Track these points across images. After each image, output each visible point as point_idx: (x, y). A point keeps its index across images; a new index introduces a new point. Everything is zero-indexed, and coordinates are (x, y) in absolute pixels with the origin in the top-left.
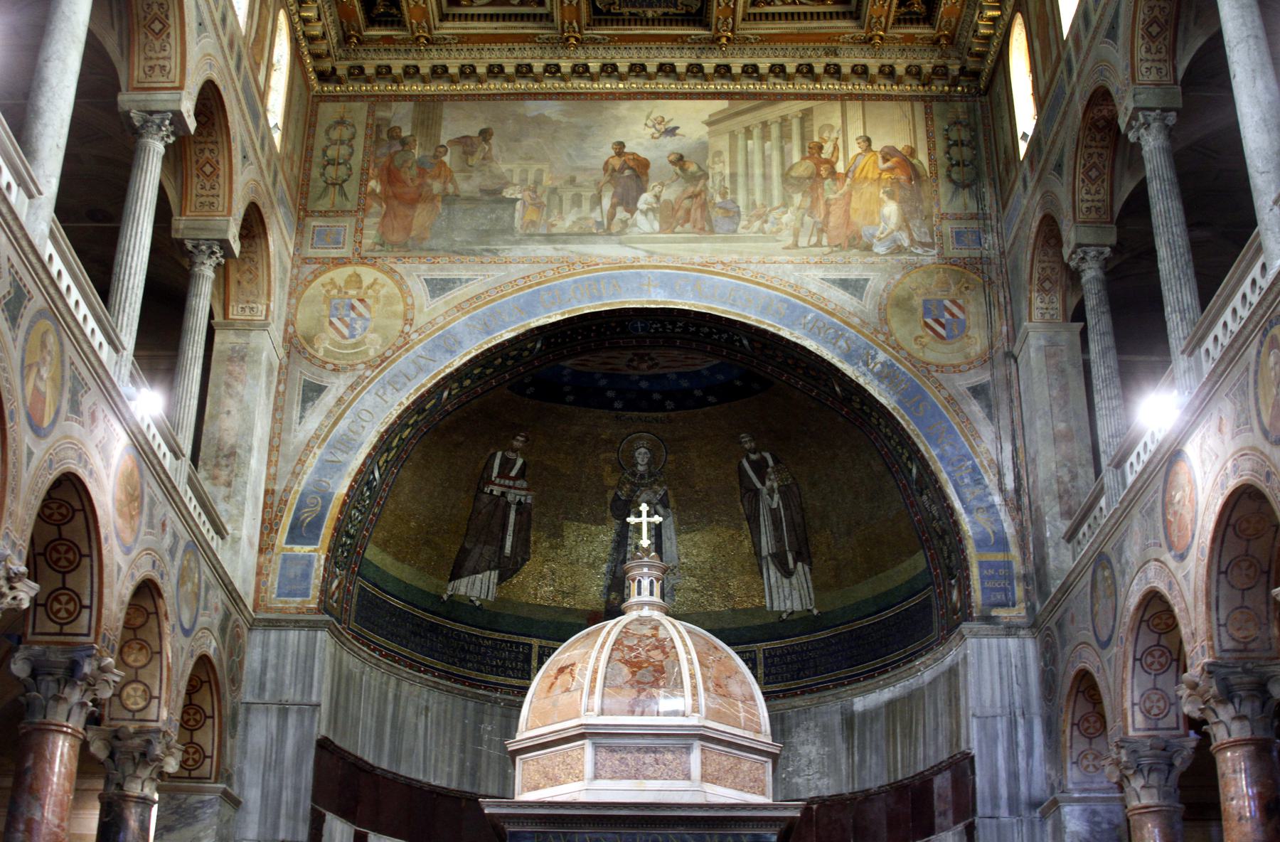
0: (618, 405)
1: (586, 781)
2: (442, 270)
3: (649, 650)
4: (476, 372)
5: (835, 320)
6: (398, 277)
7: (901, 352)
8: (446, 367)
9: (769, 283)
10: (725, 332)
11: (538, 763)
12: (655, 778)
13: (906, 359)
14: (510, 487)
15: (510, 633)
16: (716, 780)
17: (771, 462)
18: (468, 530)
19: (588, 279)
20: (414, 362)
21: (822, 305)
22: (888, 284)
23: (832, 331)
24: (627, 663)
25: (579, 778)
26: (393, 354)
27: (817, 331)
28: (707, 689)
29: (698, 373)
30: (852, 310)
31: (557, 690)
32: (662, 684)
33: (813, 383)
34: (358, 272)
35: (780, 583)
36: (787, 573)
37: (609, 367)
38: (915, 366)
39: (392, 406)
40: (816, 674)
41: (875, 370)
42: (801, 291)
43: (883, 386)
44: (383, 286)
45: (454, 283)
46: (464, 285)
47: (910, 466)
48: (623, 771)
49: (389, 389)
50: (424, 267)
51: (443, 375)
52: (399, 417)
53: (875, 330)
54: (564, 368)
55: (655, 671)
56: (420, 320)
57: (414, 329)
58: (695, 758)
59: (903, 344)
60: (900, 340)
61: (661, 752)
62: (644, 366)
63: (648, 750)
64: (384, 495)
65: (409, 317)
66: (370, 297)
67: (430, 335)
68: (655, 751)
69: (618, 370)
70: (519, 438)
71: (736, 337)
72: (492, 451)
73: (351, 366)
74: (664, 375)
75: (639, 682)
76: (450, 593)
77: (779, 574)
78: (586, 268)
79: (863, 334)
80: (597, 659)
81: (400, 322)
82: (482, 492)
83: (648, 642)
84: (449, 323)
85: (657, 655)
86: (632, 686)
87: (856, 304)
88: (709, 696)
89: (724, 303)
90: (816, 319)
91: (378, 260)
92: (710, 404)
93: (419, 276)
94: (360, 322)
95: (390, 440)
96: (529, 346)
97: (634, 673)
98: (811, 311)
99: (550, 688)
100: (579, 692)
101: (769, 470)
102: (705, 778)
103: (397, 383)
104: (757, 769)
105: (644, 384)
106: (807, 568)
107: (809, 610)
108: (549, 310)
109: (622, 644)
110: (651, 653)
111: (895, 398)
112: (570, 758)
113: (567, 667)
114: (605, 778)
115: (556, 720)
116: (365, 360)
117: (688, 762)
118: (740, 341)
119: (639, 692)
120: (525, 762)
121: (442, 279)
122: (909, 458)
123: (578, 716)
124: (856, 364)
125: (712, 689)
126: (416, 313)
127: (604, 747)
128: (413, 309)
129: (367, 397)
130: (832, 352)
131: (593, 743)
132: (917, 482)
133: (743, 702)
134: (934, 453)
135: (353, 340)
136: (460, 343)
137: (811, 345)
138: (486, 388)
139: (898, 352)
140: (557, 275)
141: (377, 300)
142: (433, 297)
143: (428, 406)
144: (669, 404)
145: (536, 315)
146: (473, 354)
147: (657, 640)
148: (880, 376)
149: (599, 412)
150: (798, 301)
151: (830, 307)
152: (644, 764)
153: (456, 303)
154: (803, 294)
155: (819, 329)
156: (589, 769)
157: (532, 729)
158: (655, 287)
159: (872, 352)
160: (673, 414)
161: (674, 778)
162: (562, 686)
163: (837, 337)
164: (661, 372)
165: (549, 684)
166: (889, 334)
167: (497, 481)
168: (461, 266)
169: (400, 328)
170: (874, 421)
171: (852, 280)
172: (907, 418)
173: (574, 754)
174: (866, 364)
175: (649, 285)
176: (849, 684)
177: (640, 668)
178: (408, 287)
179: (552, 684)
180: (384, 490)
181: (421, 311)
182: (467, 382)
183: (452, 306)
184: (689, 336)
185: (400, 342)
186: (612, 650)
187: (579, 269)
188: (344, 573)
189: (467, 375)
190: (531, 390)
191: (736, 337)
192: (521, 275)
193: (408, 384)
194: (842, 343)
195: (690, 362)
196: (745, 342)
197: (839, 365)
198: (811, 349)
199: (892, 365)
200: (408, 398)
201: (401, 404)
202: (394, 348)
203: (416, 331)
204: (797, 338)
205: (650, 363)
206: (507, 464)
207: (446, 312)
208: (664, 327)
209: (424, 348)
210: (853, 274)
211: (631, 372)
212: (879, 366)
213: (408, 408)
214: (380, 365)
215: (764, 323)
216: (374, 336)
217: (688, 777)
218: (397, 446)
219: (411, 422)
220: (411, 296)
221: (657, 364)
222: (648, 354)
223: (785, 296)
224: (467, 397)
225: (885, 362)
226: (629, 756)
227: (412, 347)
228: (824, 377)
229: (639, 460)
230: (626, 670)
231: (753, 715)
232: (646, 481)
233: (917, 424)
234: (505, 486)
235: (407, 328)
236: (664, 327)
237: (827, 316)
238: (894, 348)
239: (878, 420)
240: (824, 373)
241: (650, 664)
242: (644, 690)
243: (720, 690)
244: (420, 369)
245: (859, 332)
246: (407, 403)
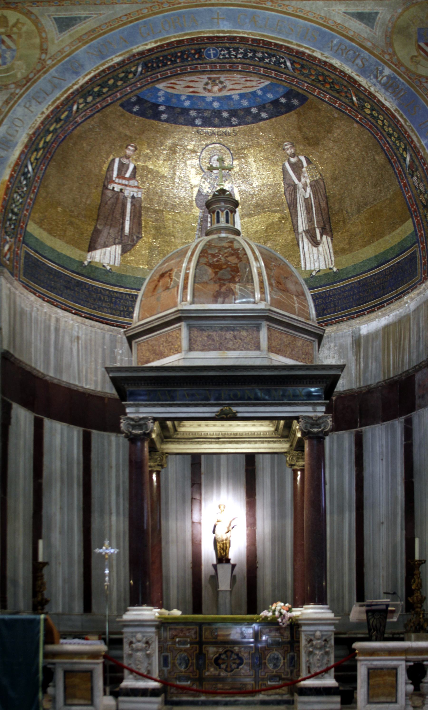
0: (198, 122)
1: (183, 353)
2: (66, 11)
3: (227, 257)
4: (96, 89)
5: (354, 44)
6: (33, 17)
7: (401, 68)
8: (74, 84)
9: (305, 16)
10: (274, 56)
11: (148, 344)
12: (234, 350)
13: (404, 73)
15: (132, 289)
16: (278, 352)
18: (98, 215)
19: (173, 15)
20: (49, 81)
21: (345, 33)
22: (393, 16)
23: (351, 52)
24: (210, 265)
25: (178, 351)
26: (35, 76)
27: (340, 52)
28: (270, 285)
29: (254, 94)
30: (366, 36)
31: (160, 290)
32: (237, 280)
33: (337, 95)
34: (5, 15)
37: (191, 90)
38: (411, 79)
39: (36, 115)
40: (335, 312)
41: (382, 81)
42: (330, 22)
43: (388, 94)
44: (24, 24)
45: (76, 20)
46: (83, 22)
47: (405, 156)
48: (210, 344)
49: (34, 102)
50: (52, 9)
51: (71, 91)
52: (42, 123)
53: (383, 51)
54: (159, 90)
55: (232, 271)
56: (53, 49)
57: (48, 56)
58: (264, 334)
59: (403, 61)
60: (401, 58)
61: (238, 330)
63: (228, 329)
64: (37, 185)
65: (45, 47)
66: (14, 33)
67: (60, 61)
68: (234, 329)
69: (197, 92)
71: (282, 60)
72: (111, 157)
73: (5, 86)
74: (229, 98)
75: (220, 279)
78: (172, 7)
79: (375, 55)
80: (188, 268)
81: (38, 51)
83: (226, 251)
84: (73, 51)
85: (233, 260)
86: (215, 282)
87: (369, 31)
88: (272, 289)
89: (273, 31)
90: (340, 43)
91: (19, 4)
92: (264, 119)
93: (49, 16)
94: (9, 53)
95: (37, 141)
96: (133, 70)
97: (216, 273)
98: (337, 37)
99: (155, 289)
100: (176, 289)
102: (270, 349)
103: (39, 97)
104: (307, 346)
105: (216, 105)
108: (145, 39)
109: (206, 252)
110: (229, 259)
111: (396, 102)
112: (171, 338)
113: (166, 272)
114: (197, 350)
115: (160, 310)
116: (15, 81)
117: (258, 338)
118: (285, 63)
119: (221, 286)
120: (138, 344)
121: (66, 18)
122: (405, 150)
123: (176, 306)
124: (369, 77)
125: (274, 285)
126: (49, 44)
127: (196, 327)
128: (47, 41)
129: (18, 108)
130: (352, 68)
131: (188, 325)
132: (410, 167)
133: (297, 296)
134: (423, 143)
135: (5, 67)
136: (82, 66)
137: (336, 62)
138: (104, 104)
139: (399, 68)
140: (151, 12)
141: (20, 35)
142: (61, 32)
143: (63, 117)
144: (234, 120)
145: (137, 43)
146: (92, 74)
147: (233, 250)
148: (386, 86)
149: (185, 128)
150: (327, 30)
151: (350, 34)
152: (226, 339)
153: (78, 36)
154: (330, 24)
155: (342, 50)
156: (185, 343)
157: (143, 319)
158: (223, 19)
159: (380, 68)
160: (237, 129)
161: (248, 349)
162: (163, 286)
163: (356, 57)
164: (228, 94)
165: (154, 286)
166: (394, 54)
168: (79, 7)
169: (38, 56)
170: (380, 122)
171: (366, 13)
172: (405, 117)
173: (174, 334)
174: (376, 77)
175: (218, 19)
176: (357, 317)
177: (221, 269)
178: (42, 24)
179: (156, 286)
180: (37, 182)
181: (53, 43)
182: (90, 99)
183: (75, 38)
184: (248, 61)
185: (39, 67)
186: (200, 257)
187: (166, 6)
188: (13, 240)
189: (89, 92)
190: (136, 108)
191: (282, 60)
192: (125, 12)
193: (47, 98)
194: (358, 61)
195: (249, 84)
196: (288, 64)
197: (357, 78)
198: (337, 66)
199: (395, 78)
200: (47, 109)
201: (43, 113)
202: (35, 71)
203: (50, 58)
204: (327, 58)
206: (123, 167)
207: (71, 43)
209: (57, 71)
210: (367, 8)
211: (206, 94)
212: (385, 78)
213: (48, 116)
214: (26, 84)
215: (302, 47)
216: (19, 63)
217: (258, 348)
218: (43, 148)
219: (52, 129)
220: (45, 31)
222: (218, 78)
223: (317, 26)
224: (91, 111)
225: (390, 75)
226: (214, 334)
227: (48, 70)
228: (346, 90)
230: (210, 271)
231: (304, 306)
233: (411, 121)
235: (43, 56)
237: (348, 41)
238: (396, 65)
239: (383, 121)
240: (345, 87)
241: (228, 266)
242: (224, 285)
243: (280, 286)
244: (55, 87)
245: (371, 52)
246: (47, 112)
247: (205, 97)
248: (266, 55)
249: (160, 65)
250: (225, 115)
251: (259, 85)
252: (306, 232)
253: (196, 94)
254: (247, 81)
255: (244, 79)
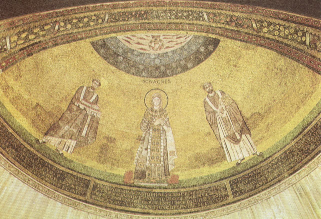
14: (89, 107)
17: (220, 96)
35: (233, 147)
36: (236, 141)
37: (141, 47)
62: (157, 46)
69: (145, 50)
70: (95, 82)
76: (44, 140)
77: (232, 144)
82: (74, 104)
101: (220, 100)
106: (248, 136)
107: (253, 154)
118: (203, 17)
167: (83, 102)
205: (160, 44)
208: (166, 15)
221: (163, 45)
222: (159, 37)
229: (155, 104)
232: (158, 114)
234: (86, 106)
236: (166, 15)
247: (150, 54)
248: (190, 13)
249: (121, 19)
250: (163, 68)
251: (186, 40)
252: (228, 137)
253: (144, 52)
254: (177, 38)
255: (176, 37)
